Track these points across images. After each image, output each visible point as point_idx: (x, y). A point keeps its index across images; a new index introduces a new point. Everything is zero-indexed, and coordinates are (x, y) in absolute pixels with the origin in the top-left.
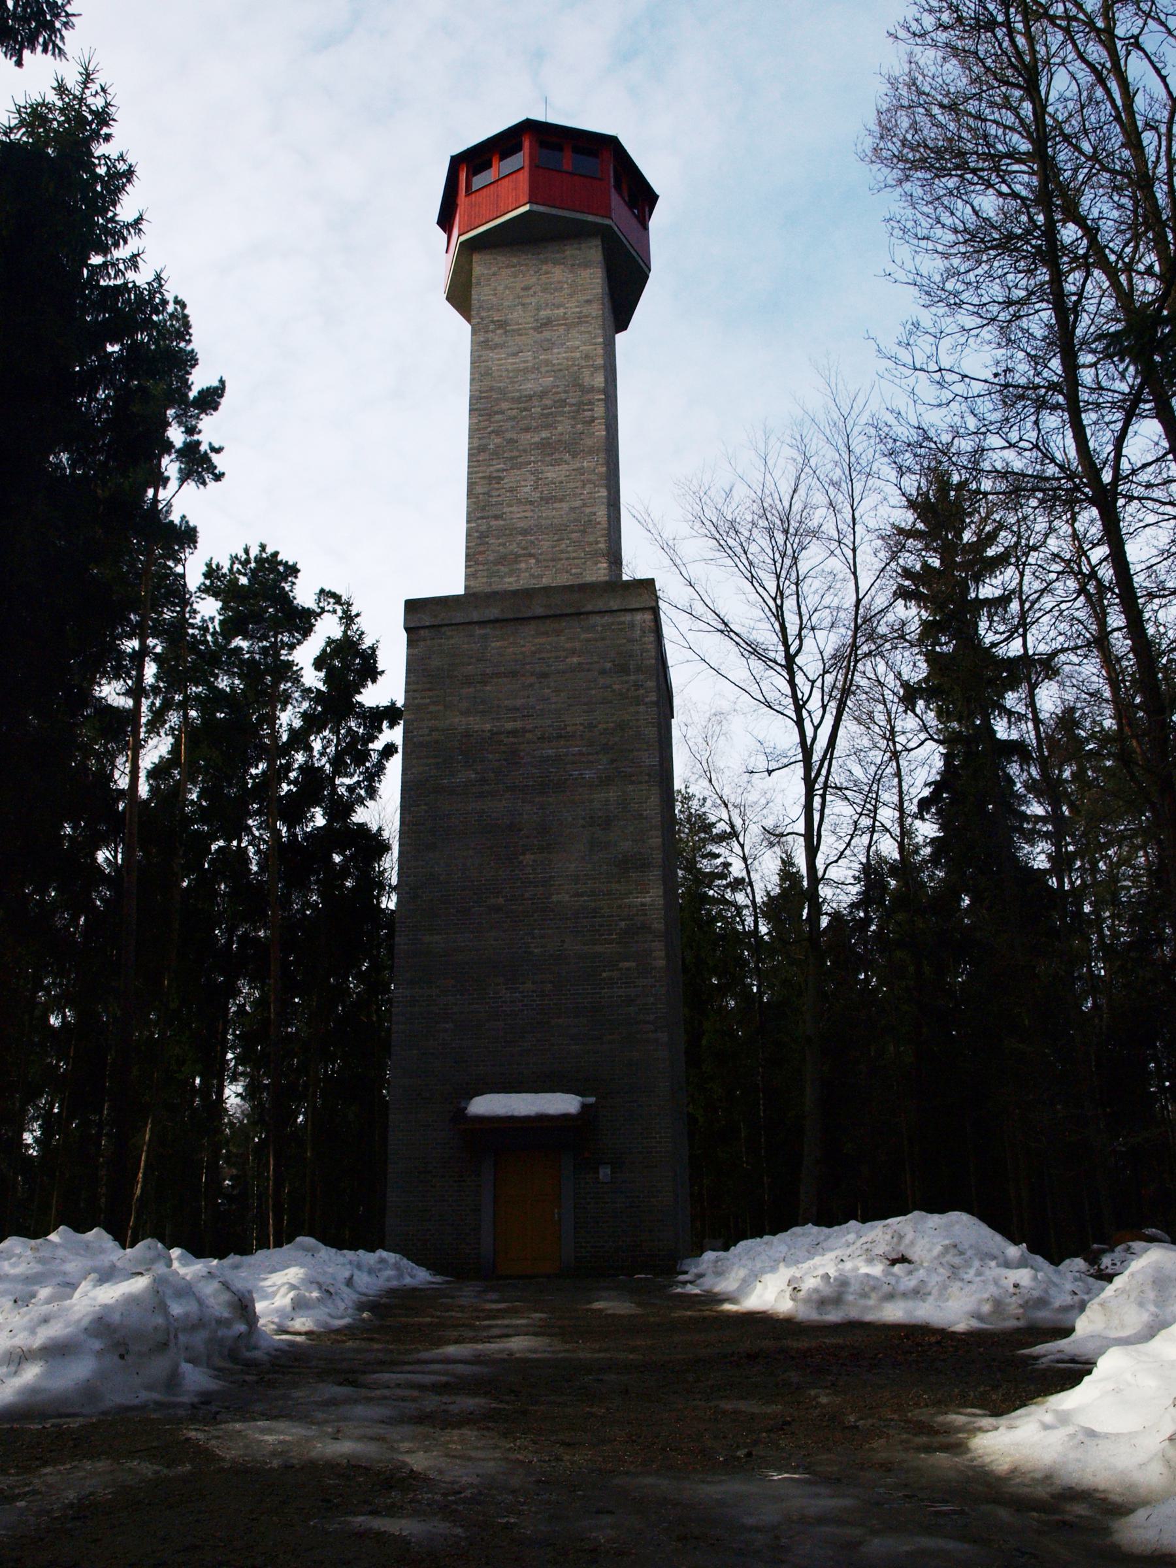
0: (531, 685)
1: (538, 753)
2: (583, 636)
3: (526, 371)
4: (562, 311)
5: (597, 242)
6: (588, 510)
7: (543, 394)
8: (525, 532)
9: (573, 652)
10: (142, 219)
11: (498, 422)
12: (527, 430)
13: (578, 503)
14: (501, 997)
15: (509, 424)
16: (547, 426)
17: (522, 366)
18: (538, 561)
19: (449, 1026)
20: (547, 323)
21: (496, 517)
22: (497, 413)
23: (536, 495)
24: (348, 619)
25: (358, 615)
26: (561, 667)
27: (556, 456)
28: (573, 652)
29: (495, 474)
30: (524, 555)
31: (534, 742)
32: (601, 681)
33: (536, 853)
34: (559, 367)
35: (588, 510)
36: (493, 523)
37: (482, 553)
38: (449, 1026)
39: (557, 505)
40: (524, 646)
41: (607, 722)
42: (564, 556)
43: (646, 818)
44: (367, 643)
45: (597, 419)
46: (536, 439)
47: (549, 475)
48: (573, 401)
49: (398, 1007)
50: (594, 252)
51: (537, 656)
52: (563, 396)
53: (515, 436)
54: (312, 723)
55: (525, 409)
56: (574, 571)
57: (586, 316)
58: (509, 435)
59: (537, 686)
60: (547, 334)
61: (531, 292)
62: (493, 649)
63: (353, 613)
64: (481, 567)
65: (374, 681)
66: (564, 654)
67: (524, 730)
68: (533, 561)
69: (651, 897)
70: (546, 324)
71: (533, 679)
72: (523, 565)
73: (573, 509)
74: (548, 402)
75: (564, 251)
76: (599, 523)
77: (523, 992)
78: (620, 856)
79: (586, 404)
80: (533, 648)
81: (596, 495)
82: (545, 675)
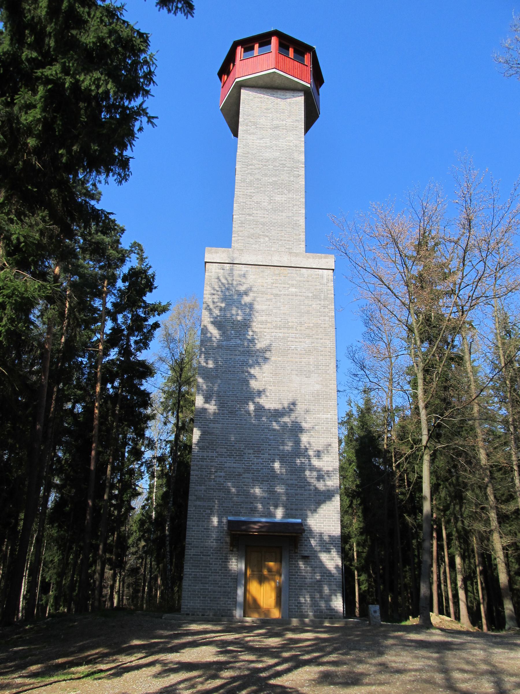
0: (271, 300)
1: (273, 334)
2: (298, 278)
3: (266, 147)
4: (284, 122)
5: (302, 94)
6: (295, 218)
7: (275, 159)
8: (263, 224)
9: (293, 285)
10: (123, 8)
11: (251, 169)
12: (266, 175)
13: (291, 214)
14: (251, 461)
15: (257, 171)
16: (276, 176)
17: (264, 145)
18: (270, 239)
19: (222, 474)
20: (277, 127)
21: (250, 215)
22: (251, 165)
23: (270, 207)
24: (142, 259)
25: (146, 258)
26: (286, 292)
27: (280, 190)
28: (293, 285)
29: (249, 194)
30: (263, 236)
31: (271, 329)
32: (306, 302)
33: (271, 386)
34: (283, 149)
35: (295, 218)
36: (247, 217)
37: (242, 231)
38: (222, 474)
39: (280, 213)
40: (267, 279)
41: (309, 323)
42: (283, 238)
43: (329, 374)
44: (150, 272)
45: (300, 175)
46: (271, 181)
47: (276, 198)
48: (289, 166)
49: (194, 461)
50: (300, 100)
51: (274, 285)
52: (284, 162)
53: (260, 177)
54: (119, 308)
55: (265, 166)
56: (287, 247)
57: (296, 127)
58: (257, 176)
59: (274, 300)
60: (277, 132)
61: (269, 111)
62: (251, 278)
63: (144, 257)
64: (240, 238)
65: (151, 291)
66: (288, 286)
67: (267, 322)
68: (267, 239)
69: (331, 415)
70: (276, 127)
71: (272, 297)
72: (262, 240)
73: (288, 217)
74: (277, 164)
75: (286, 96)
76: (300, 225)
77: (263, 459)
78: (316, 392)
79: (294, 168)
80: (272, 281)
81: (300, 212)
82: (276, 295)
